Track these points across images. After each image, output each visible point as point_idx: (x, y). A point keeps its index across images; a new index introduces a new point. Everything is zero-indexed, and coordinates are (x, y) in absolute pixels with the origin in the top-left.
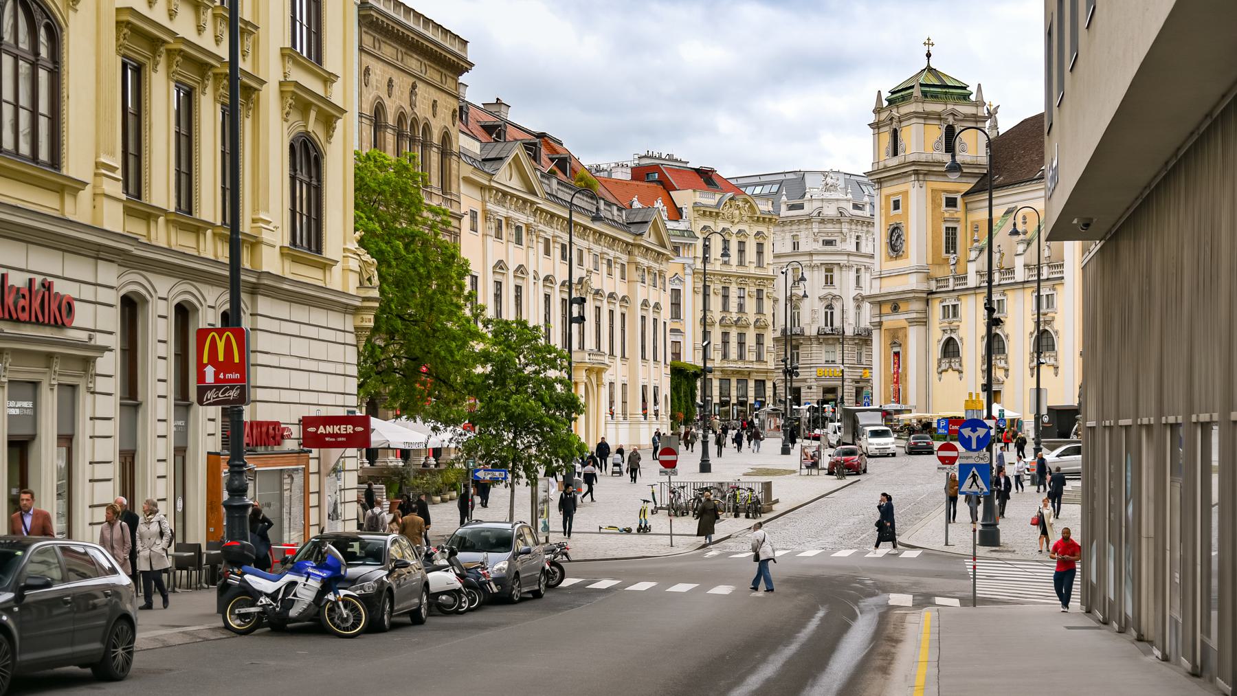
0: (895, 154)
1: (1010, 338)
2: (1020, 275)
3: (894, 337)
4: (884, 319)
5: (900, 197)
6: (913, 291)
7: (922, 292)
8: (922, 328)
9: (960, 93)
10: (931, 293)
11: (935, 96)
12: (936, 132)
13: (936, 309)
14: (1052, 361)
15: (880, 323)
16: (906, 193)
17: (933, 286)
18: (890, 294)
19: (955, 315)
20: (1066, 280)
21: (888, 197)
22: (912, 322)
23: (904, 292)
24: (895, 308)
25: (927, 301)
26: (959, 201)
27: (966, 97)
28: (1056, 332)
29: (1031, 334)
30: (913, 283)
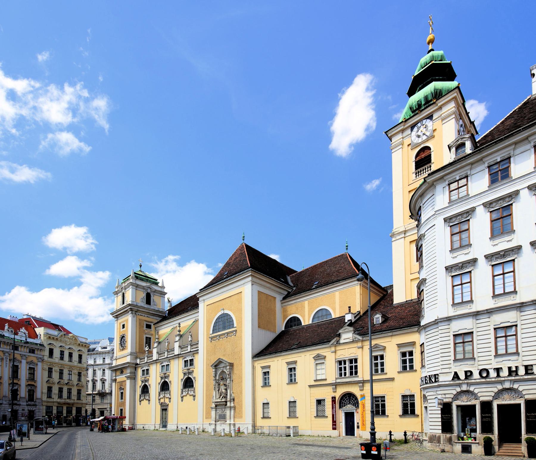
1: (172, 383)
2: (177, 351)
3: (121, 385)
4: (117, 378)
6: (128, 363)
7: (133, 364)
8: (133, 381)
10: (137, 364)
13: (140, 372)
14: (192, 393)
15: (116, 380)
17: (138, 361)
18: (119, 365)
19: (147, 374)
20: (199, 351)
22: (128, 378)
23: (124, 364)
24: (122, 372)
25: (136, 368)
28: (194, 378)
29: (182, 380)
30: (128, 359)
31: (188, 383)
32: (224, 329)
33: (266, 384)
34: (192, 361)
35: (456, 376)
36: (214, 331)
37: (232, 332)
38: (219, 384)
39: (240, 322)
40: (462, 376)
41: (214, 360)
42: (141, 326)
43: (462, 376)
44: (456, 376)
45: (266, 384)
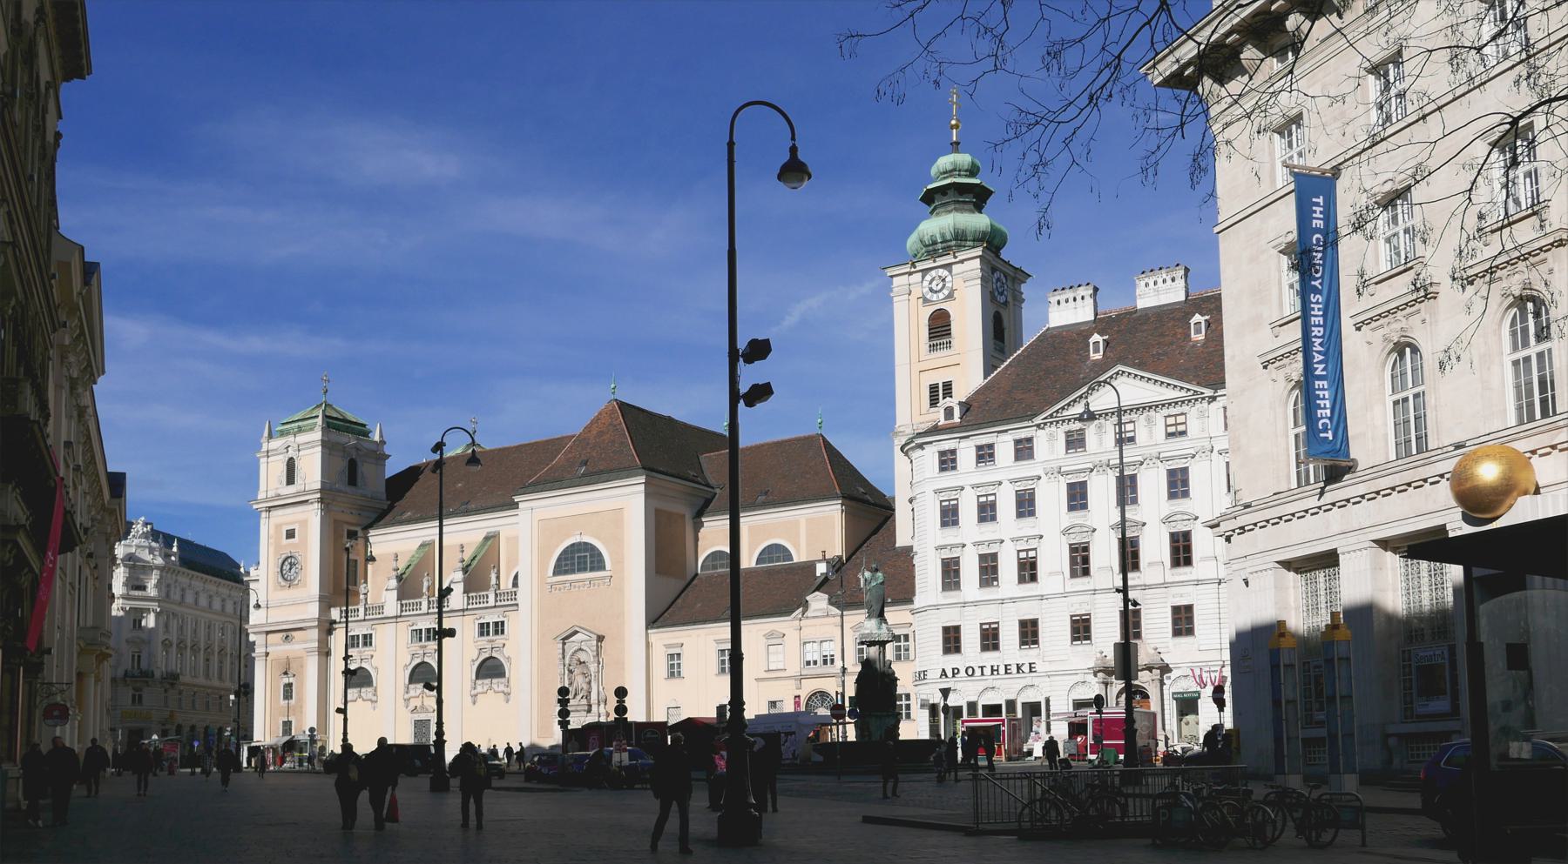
0: (290, 480)
5: (296, 527)
9: (361, 431)
11: (338, 429)
12: (342, 464)
16: (304, 523)
21: (278, 526)
23: (303, 621)
26: (360, 534)
27: (366, 434)
31: (490, 669)
32: (582, 569)
33: (674, 672)
34: (499, 628)
35: (944, 673)
36: (558, 570)
37: (603, 578)
38: (571, 672)
39: (619, 561)
40: (950, 674)
41: (564, 629)
42: (337, 536)
43: (950, 674)
44: (944, 673)
45: (674, 672)
